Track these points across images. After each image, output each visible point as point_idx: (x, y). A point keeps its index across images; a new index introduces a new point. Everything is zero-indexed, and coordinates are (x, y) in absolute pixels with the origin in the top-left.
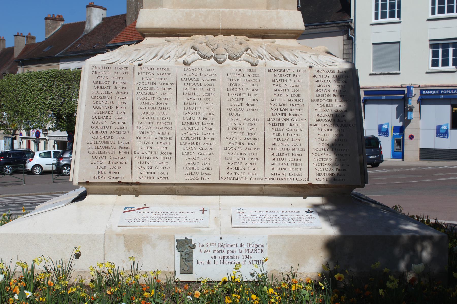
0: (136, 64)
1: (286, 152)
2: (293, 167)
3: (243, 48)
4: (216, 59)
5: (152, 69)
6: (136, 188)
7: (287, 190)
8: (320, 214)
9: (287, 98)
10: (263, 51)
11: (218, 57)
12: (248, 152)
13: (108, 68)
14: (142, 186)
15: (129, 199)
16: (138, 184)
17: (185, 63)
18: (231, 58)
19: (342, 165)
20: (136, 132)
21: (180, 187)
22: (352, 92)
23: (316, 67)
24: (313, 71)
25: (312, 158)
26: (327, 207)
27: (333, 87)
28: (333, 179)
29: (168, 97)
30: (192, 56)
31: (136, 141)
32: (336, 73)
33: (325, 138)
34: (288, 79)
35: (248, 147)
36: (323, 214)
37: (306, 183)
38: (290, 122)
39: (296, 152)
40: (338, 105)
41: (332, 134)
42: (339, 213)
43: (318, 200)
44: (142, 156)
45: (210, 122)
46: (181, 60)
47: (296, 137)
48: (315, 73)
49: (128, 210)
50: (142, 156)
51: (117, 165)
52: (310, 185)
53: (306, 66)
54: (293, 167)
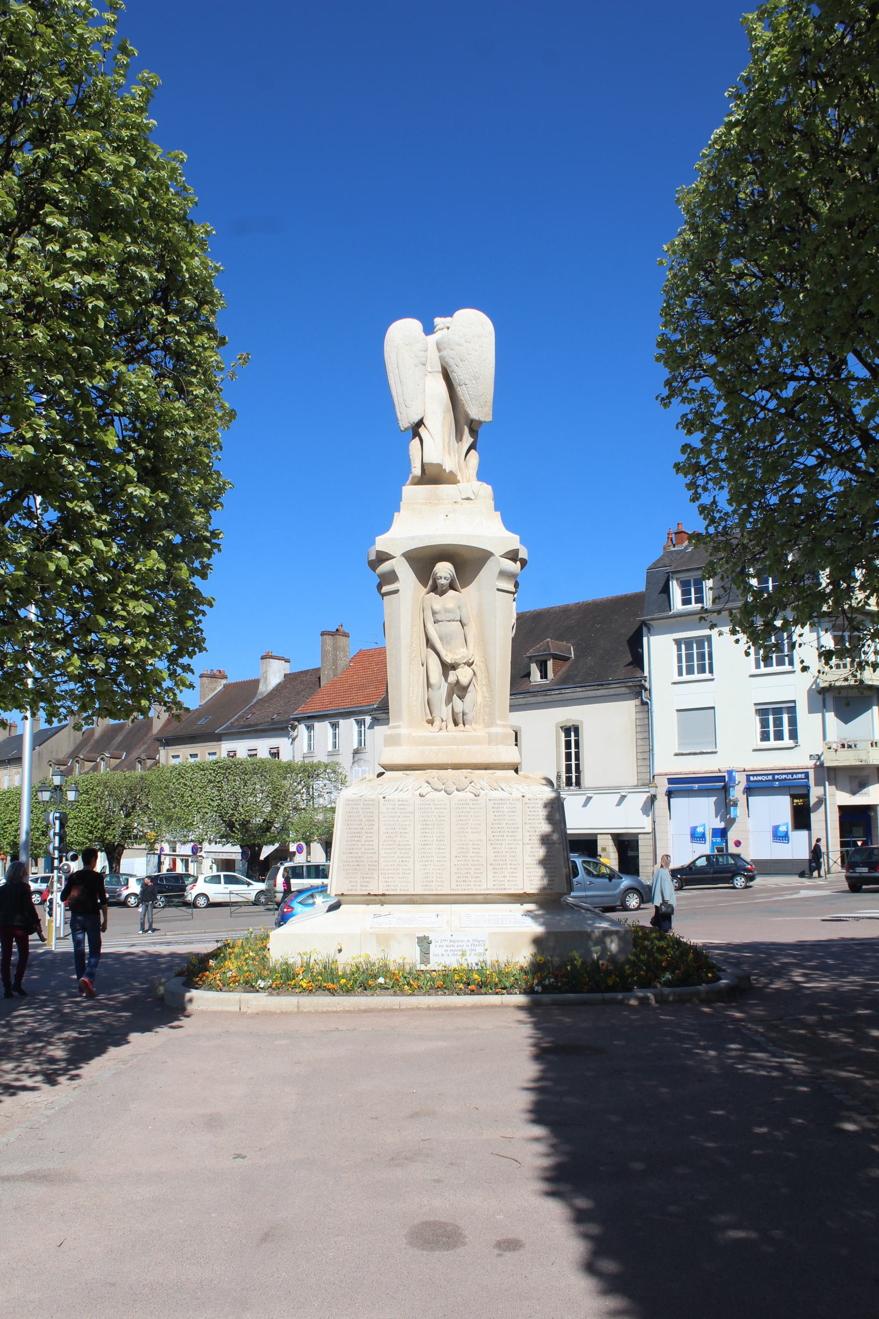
0: (381, 796)
1: (504, 867)
2: (511, 879)
3: (468, 781)
4: (445, 791)
5: (394, 801)
6: (382, 899)
7: (506, 898)
8: (532, 917)
9: (504, 822)
10: (484, 784)
11: (448, 789)
12: (473, 868)
13: (358, 800)
14: (387, 897)
15: (377, 907)
16: (384, 895)
17: (421, 796)
18: (458, 790)
19: (550, 877)
20: (381, 852)
21: (418, 897)
22: (557, 816)
23: (528, 796)
24: (526, 800)
25: (526, 871)
26: (540, 912)
27: (542, 813)
28: (543, 889)
29: (407, 823)
30: (426, 789)
31: (382, 860)
32: (545, 800)
33: (536, 854)
34: (505, 806)
35: (474, 863)
36: (535, 917)
37: (522, 892)
38: (507, 842)
39: (513, 866)
40: (546, 828)
41: (541, 852)
42: (548, 916)
43: (531, 907)
44: (387, 872)
45: (442, 843)
46: (417, 793)
47: (513, 854)
48: (527, 801)
49: (376, 916)
50: (387, 872)
51: (367, 880)
52: (525, 893)
53: (520, 796)
54: (511, 879)
